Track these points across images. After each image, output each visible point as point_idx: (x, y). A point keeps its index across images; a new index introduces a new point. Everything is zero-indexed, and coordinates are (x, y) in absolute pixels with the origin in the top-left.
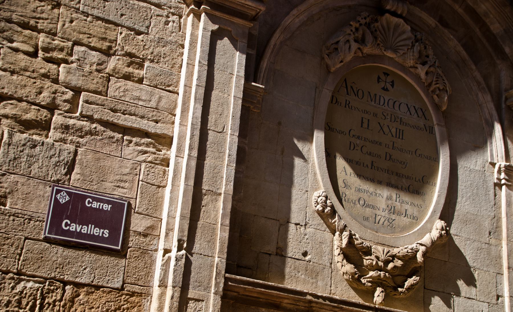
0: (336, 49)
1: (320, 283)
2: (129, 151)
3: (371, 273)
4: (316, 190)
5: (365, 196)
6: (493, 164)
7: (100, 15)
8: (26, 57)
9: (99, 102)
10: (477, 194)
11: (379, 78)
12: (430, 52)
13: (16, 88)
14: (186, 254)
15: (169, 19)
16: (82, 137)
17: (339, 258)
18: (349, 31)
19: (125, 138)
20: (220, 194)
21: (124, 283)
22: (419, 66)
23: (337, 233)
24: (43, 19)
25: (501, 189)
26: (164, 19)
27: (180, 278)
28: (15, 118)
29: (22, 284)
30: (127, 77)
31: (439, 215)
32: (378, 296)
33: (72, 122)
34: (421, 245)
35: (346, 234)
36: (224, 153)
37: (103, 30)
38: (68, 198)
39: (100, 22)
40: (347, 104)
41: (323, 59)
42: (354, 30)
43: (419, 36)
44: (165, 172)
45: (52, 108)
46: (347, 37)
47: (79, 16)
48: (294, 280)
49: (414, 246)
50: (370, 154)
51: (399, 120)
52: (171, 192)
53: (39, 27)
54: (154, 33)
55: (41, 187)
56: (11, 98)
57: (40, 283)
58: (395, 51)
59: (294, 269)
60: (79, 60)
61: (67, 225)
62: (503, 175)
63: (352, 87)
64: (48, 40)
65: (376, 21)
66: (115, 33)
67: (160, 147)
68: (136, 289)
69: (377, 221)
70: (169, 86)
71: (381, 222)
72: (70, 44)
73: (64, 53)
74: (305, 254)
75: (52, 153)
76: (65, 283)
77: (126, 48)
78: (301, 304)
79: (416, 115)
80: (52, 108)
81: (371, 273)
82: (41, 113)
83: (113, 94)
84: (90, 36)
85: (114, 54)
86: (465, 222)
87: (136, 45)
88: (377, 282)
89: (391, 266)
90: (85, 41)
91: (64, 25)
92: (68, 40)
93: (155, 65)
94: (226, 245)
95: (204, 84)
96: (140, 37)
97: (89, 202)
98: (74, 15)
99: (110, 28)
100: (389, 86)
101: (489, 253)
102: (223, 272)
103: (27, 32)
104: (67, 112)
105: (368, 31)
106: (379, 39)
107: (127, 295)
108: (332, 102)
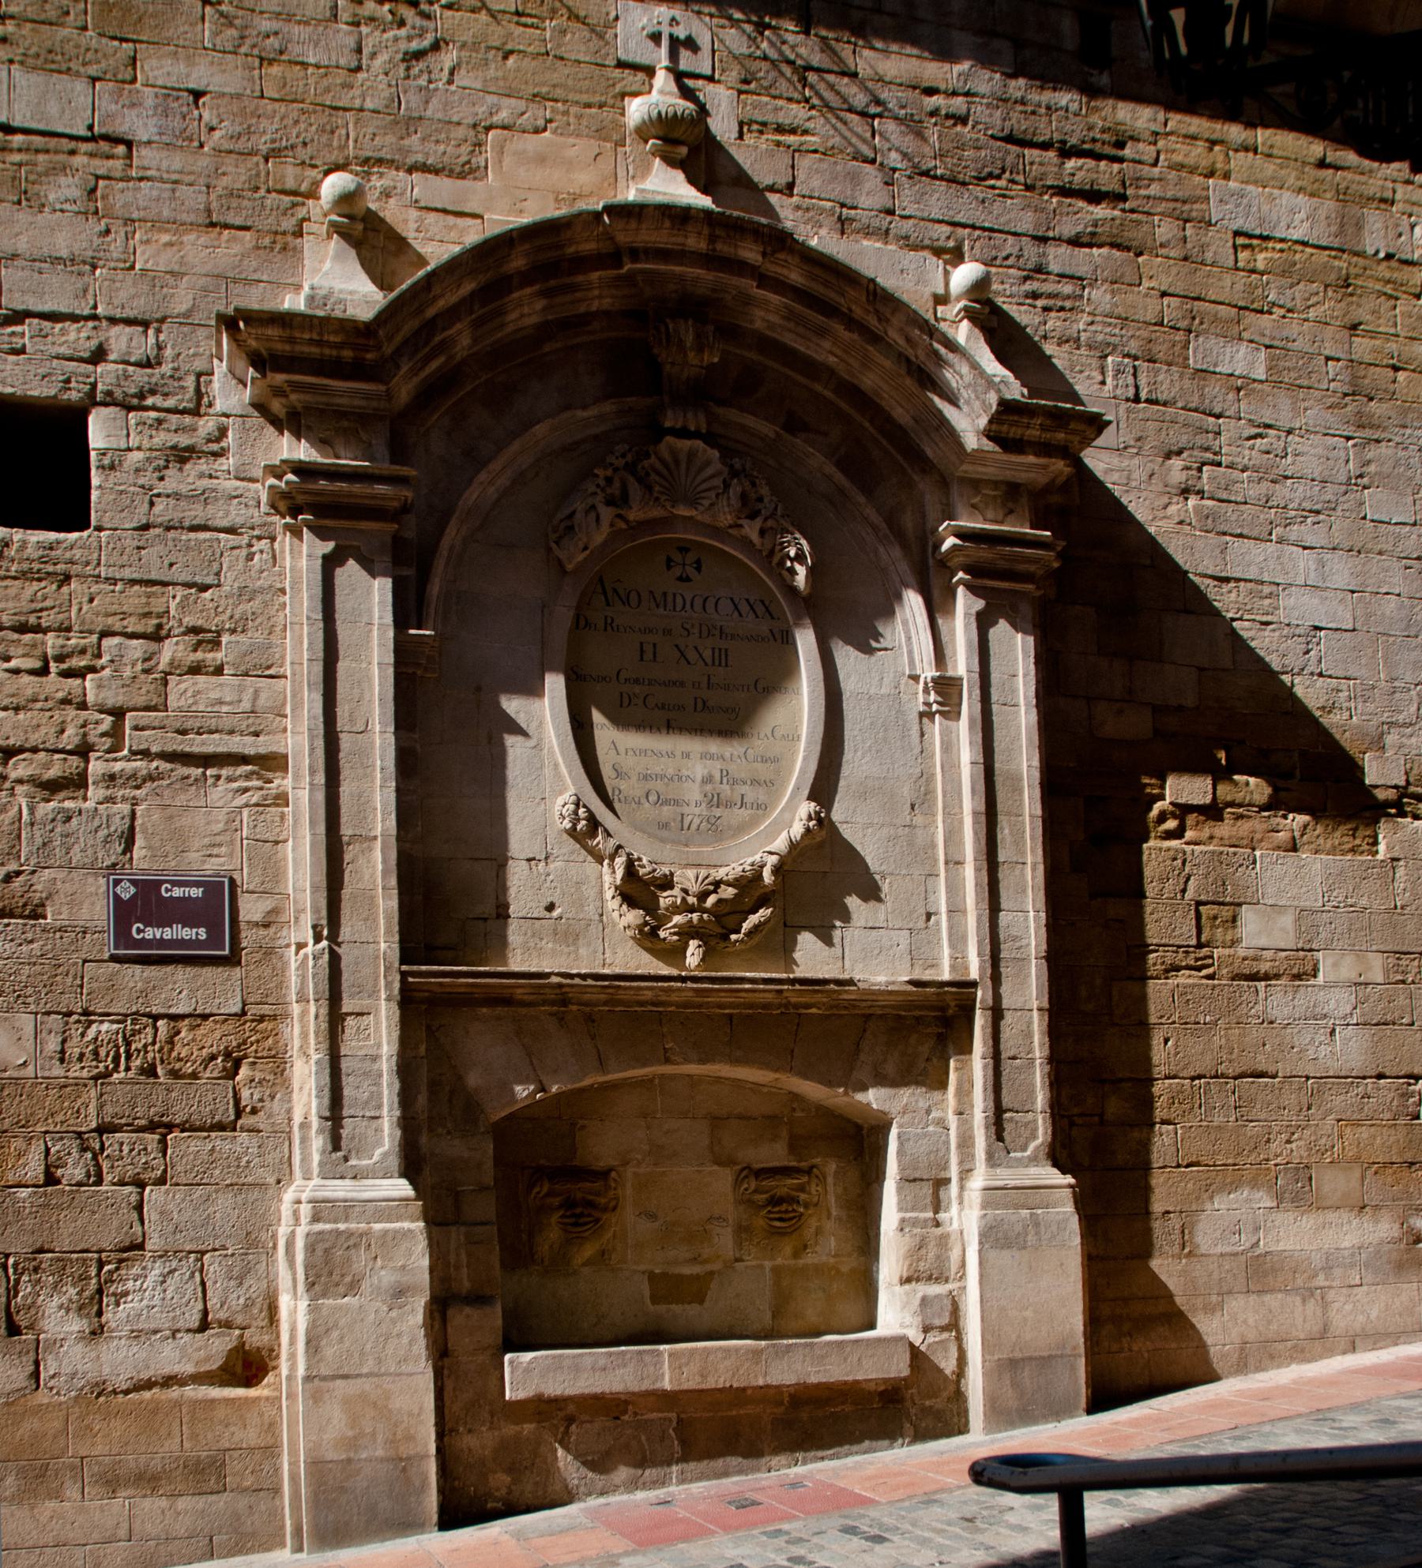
0: (571, 528)
1: (583, 951)
2: (219, 793)
3: (677, 919)
4: (561, 793)
5: (659, 785)
6: (915, 678)
7: (135, 576)
8: (32, 678)
9: (156, 724)
10: (885, 740)
11: (669, 560)
12: (765, 491)
13: (26, 732)
14: (330, 947)
15: (254, 549)
16: (138, 787)
17: (613, 904)
18: (592, 489)
19: (208, 773)
20: (375, 838)
21: (244, 1004)
22: (745, 522)
23: (606, 862)
24: (47, 609)
25: (933, 722)
26: (244, 552)
27: (325, 986)
28: (33, 781)
29: (94, 1027)
30: (195, 670)
31: (806, 792)
32: (693, 954)
33: (118, 766)
34: (771, 853)
35: (620, 861)
36: (374, 766)
37: (144, 600)
38: (133, 890)
39: (137, 588)
40: (609, 624)
41: (549, 550)
42: (602, 483)
43: (738, 466)
44: (283, 816)
45: (83, 751)
46: (590, 501)
47: (102, 586)
48: (535, 954)
49: (757, 858)
50: (663, 708)
51: (717, 633)
52: (293, 850)
53: (44, 625)
54: (229, 581)
55: (91, 880)
56: (21, 750)
57: (118, 1022)
58: (693, 503)
59: (533, 935)
60: (112, 661)
61: (139, 931)
62: (932, 697)
63: (615, 590)
64: (61, 642)
65: (647, 456)
66: (165, 599)
67: (270, 775)
68: (266, 1009)
69: (686, 826)
70: (269, 667)
71: (694, 826)
72: (94, 638)
73: (88, 656)
74: (550, 907)
75: (96, 823)
76: (156, 1018)
77: (186, 621)
78: (547, 990)
79: (751, 615)
80: (83, 751)
81: (677, 919)
82: (69, 763)
83: (175, 705)
84: (124, 615)
85: (168, 636)
86: (863, 794)
87: (202, 611)
88: (687, 933)
89: (711, 900)
90: (117, 627)
91: (80, 609)
92: (91, 632)
93: (241, 638)
94: (396, 920)
95: (321, 655)
96: (207, 595)
97: (167, 890)
98: (94, 588)
99: (154, 593)
100: (690, 571)
101: (911, 844)
102: (397, 964)
103: (28, 637)
104: (108, 752)
105: (631, 479)
106: (657, 488)
107: (253, 1021)
108: (577, 627)
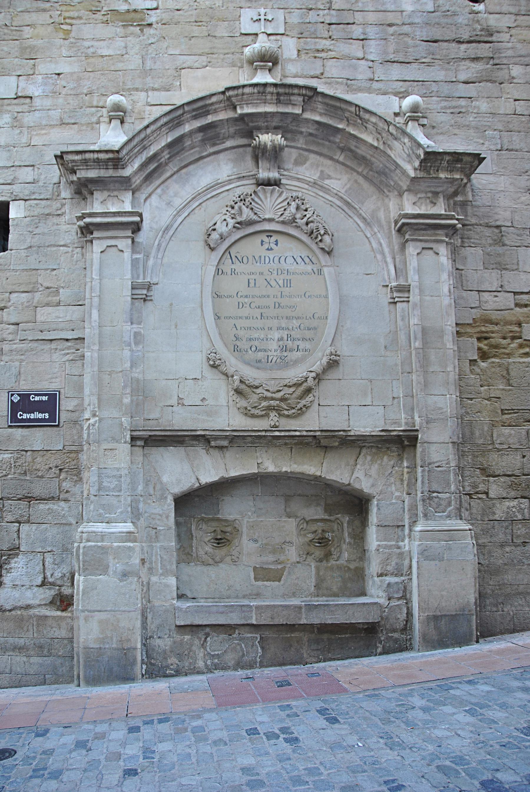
5: (256, 343)
9: (31, 328)
11: (262, 241)
26: (70, 254)
30: (48, 305)
38: (19, 398)
40: (233, 272)
51: (286, 272)
61: (21, 415)
69: (270, 361)
71: (274, 361)
97: (33, 398)
98: (8, 274)
100: (273, 246)
